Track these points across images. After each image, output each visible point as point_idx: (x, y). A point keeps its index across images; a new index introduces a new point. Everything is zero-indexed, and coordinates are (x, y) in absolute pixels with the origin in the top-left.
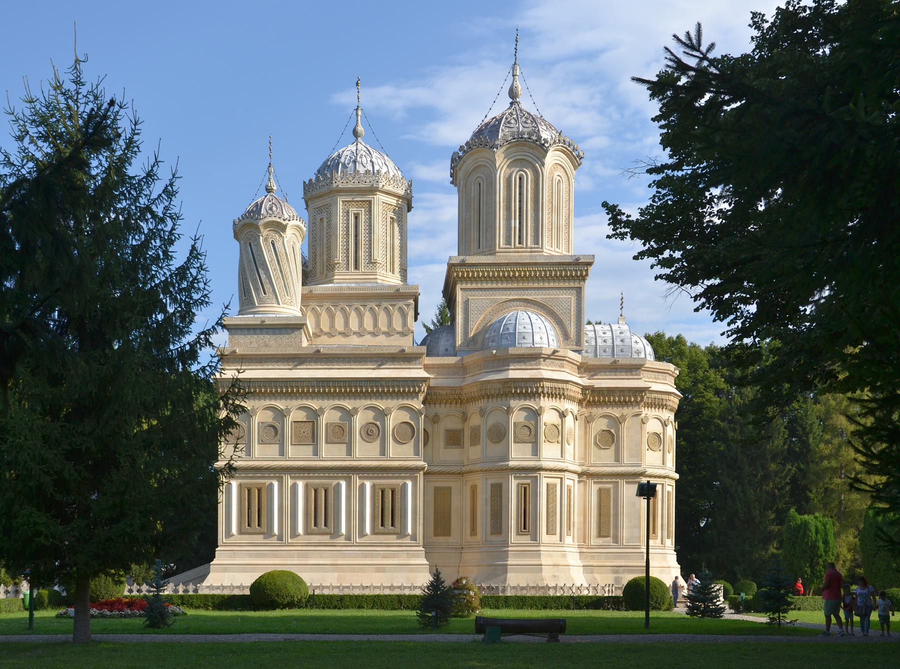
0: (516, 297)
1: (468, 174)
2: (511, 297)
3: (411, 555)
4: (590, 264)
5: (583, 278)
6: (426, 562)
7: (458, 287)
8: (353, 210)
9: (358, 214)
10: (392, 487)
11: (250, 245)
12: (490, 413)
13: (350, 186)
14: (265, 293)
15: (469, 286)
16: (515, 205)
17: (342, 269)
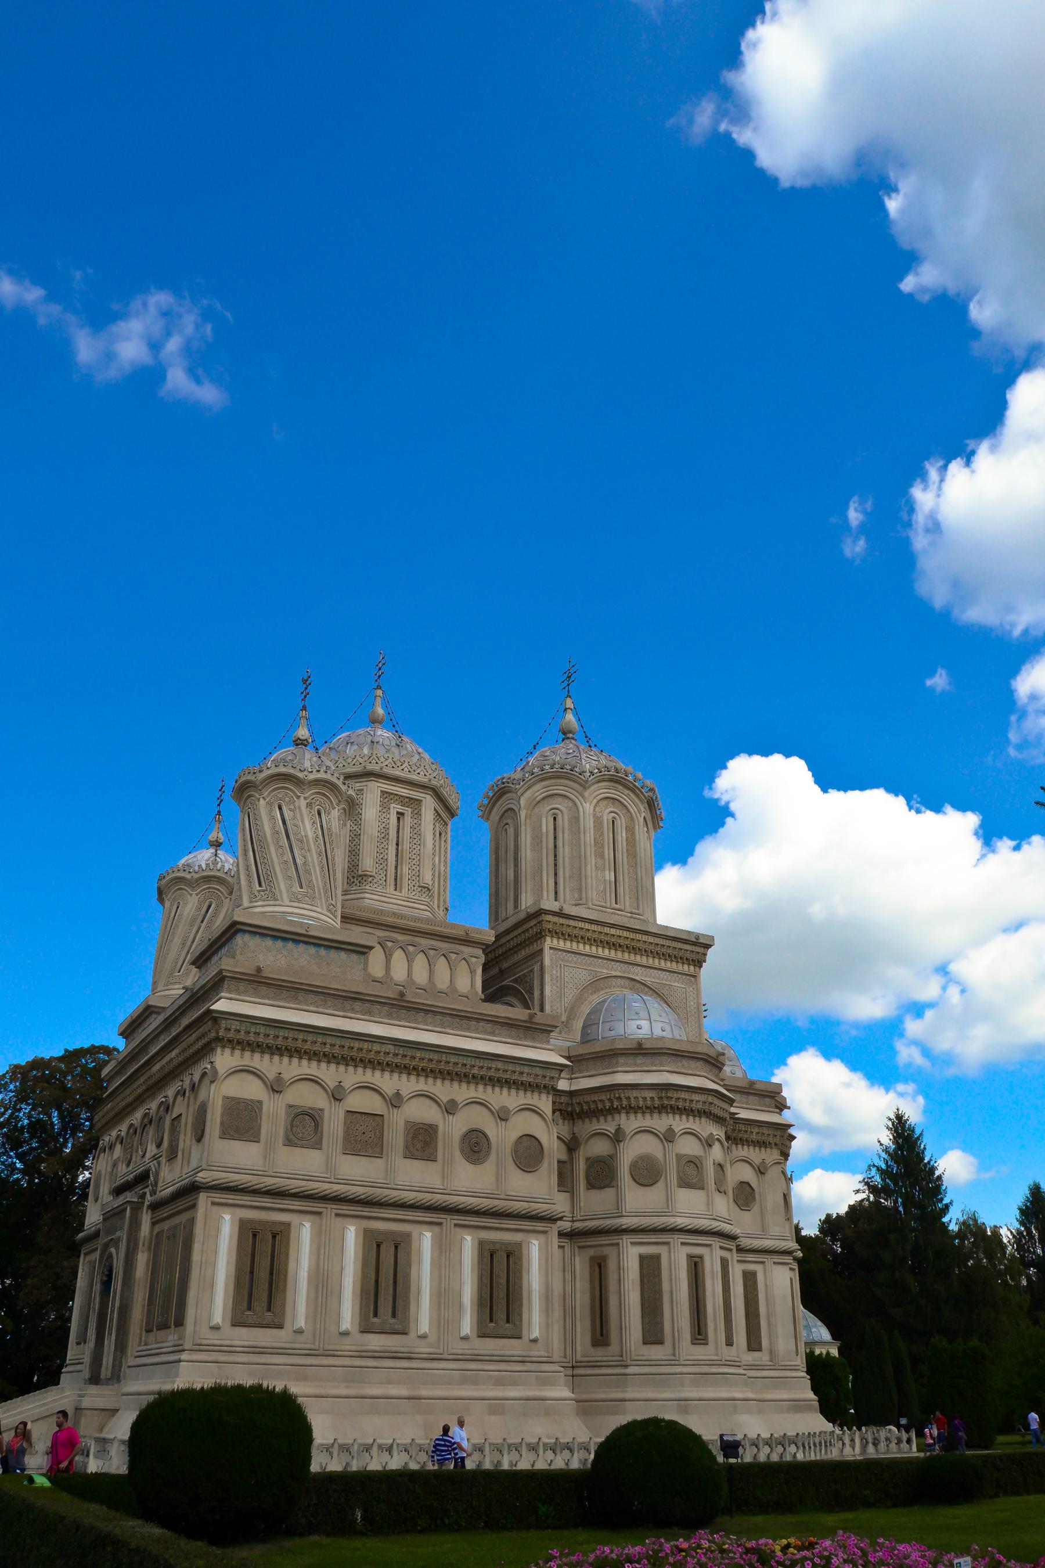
0: (620, 974)
1: (535, 802)
2: (614, 973)
3: (544, 1382)
4: (708, 946)
5: (699, 963)
6: (567, 1394)
7: (549, 942)
8: (395, 808)
9: (403, 814)
10: (510, 1248)
11: (280, 808)
12: (632, 1137)
13: (397, 773)
14: (301, 887)
15: (561, 944)
16: (608, 853)
17: (381, 887)
